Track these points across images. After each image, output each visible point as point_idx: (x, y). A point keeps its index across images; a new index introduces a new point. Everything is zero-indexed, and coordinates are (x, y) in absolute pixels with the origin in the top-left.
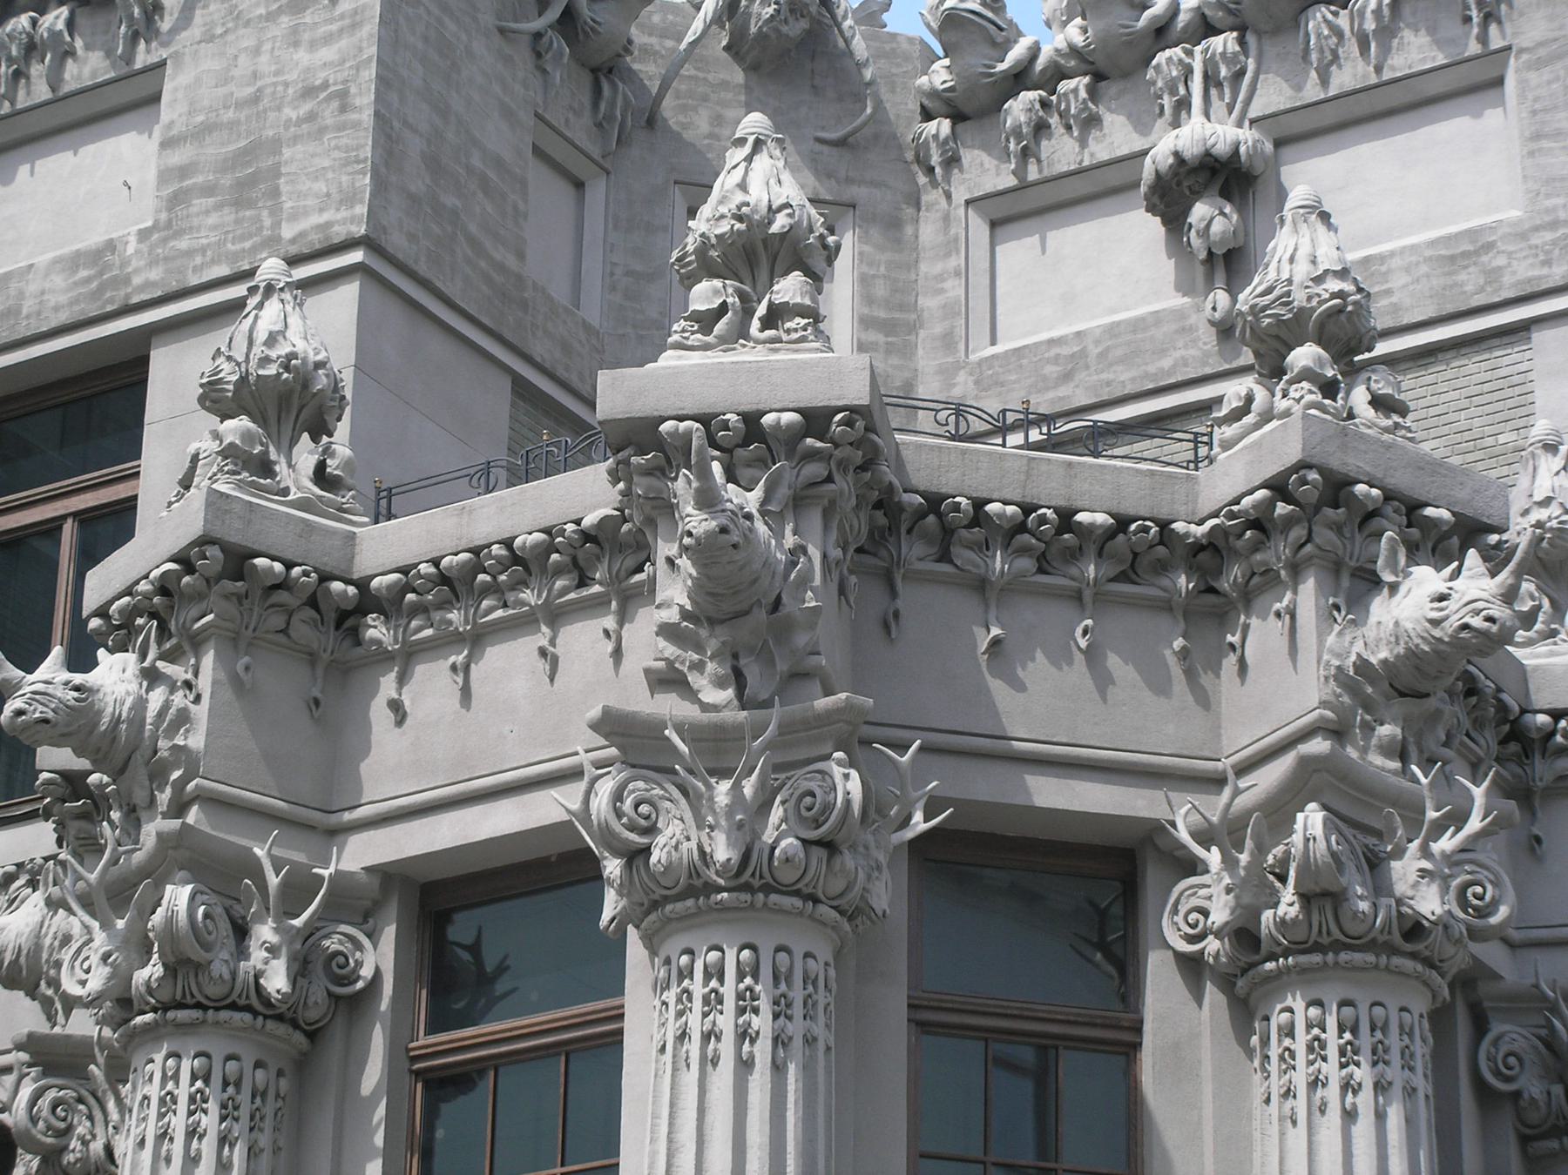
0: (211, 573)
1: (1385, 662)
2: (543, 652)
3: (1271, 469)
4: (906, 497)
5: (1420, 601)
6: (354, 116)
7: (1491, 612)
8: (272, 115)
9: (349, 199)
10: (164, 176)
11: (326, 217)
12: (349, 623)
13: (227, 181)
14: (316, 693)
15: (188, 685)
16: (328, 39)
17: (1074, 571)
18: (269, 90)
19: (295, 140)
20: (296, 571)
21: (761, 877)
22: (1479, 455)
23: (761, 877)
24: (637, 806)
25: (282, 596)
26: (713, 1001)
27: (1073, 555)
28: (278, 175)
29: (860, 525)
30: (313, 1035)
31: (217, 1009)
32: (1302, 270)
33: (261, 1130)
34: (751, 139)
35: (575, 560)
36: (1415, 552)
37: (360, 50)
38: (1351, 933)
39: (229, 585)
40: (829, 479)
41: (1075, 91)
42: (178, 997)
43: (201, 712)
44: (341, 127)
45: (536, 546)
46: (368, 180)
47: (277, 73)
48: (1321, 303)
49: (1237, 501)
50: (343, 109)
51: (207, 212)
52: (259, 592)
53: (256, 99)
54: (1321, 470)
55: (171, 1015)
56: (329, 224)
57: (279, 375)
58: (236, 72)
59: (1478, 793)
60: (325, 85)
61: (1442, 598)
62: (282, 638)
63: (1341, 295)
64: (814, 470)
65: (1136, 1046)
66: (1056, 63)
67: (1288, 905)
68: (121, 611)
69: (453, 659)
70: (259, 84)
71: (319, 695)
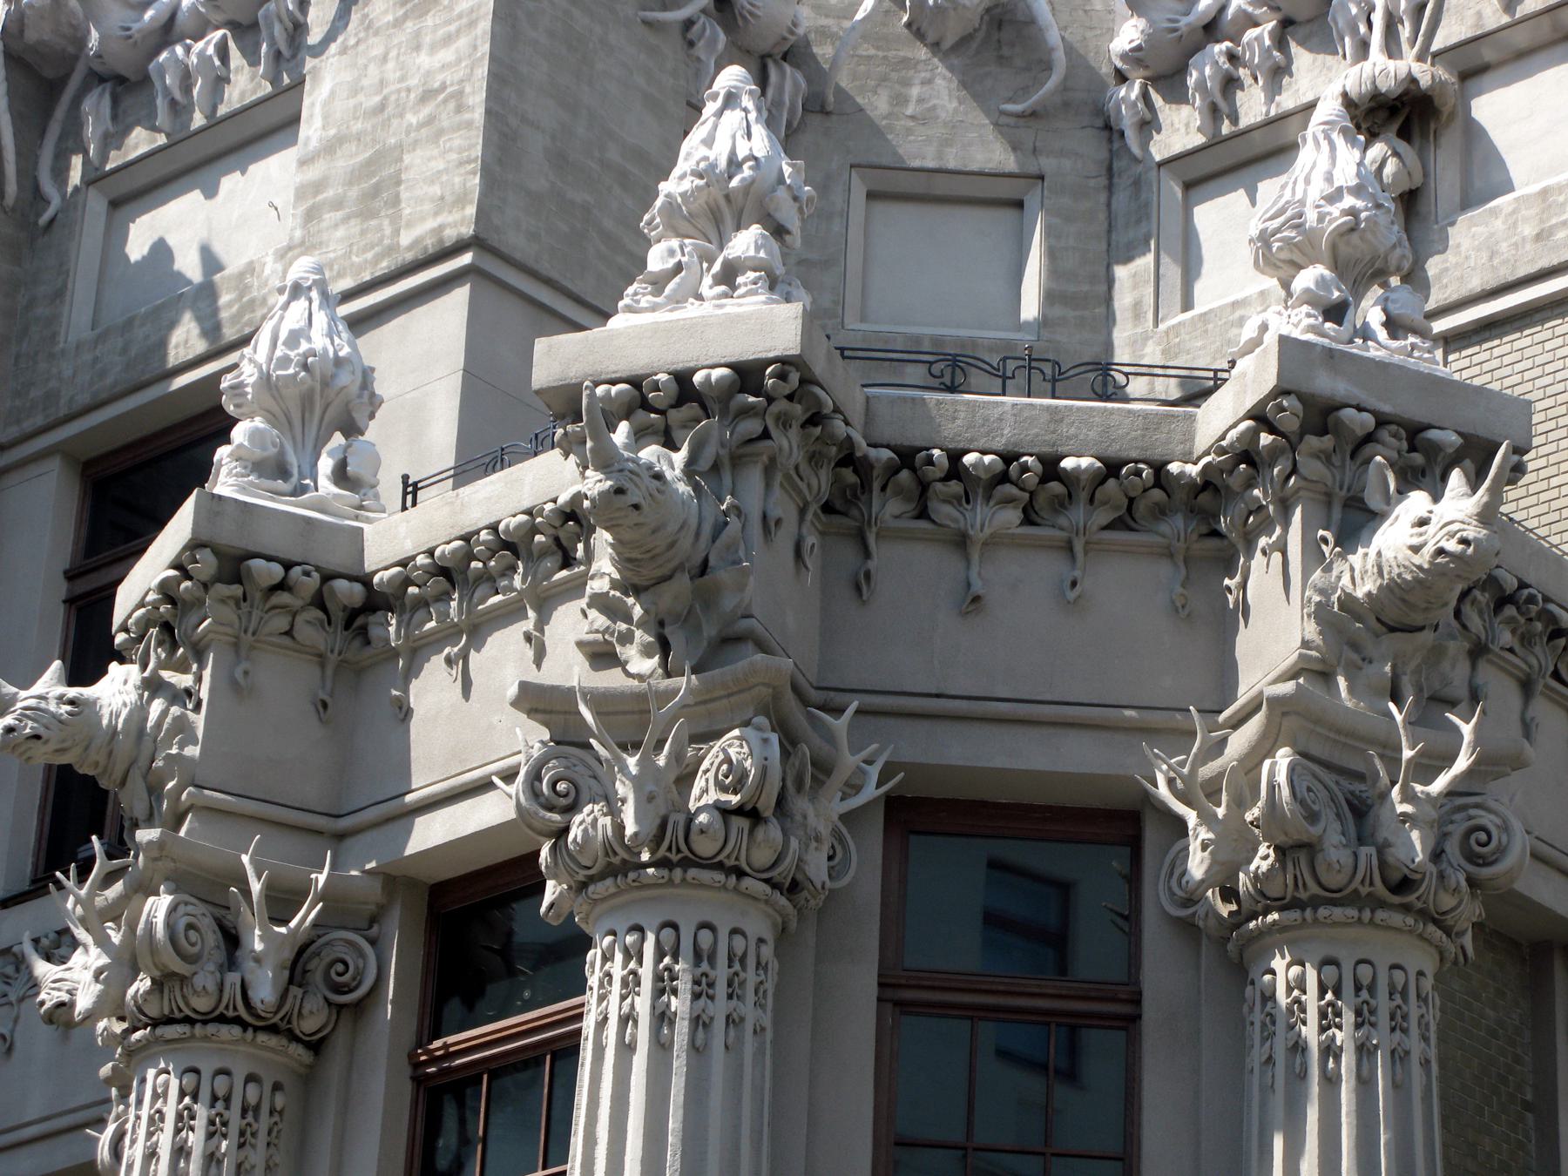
0: (204, 577)
1: (1369, 594)
2: (528, 638)
3: (1249, 402)
4: (873, 452)
5: (1421, 527)
6: (467, 116)
7: (1465, 534)
8: (395, 122)
9: (461, 201)
10: (301, 193)
11: (440, 220)
12: (359, 621)
13: (354, 193)
14: (322, 696)
15: (188, 693)
16: (448, 40)
17: (1062, 521)
18: (393, 98)
19: (416, 143)
20: (297, 570)
21: (679, 851)
22: (1476, 370)
23: (679, 851)
24: (554, 785)
25: (283, 598)
26: (631, 983)
27: (1061, 505)
28: (399, 183)
29: (821, 482)
30: (316, 1046)
31: (205, 1022)
32: (1317, 189)
33: (253, 1146)
34: (722, 93)
35: (557, 540)
36: (1411, 478)
37: (475, 48)
38: (1334, 887)
39: (222, 589)
40: (766, 435)
41: (1259, 39)
42: (166, 1012)
43: (199, 721)
44: (458, 128)
45: (519, 526)
46: (477, 180)
47: (402, 79)
48: (1330, 222)
49: (1223, 437)
50: (460, 109)
51: (336, 226)
52: (258, 595)
53: (382, 107)
54: (1301, 397)
55: (159, 1031)
56: (441, 228)
57: (297, 374)
58: (365, 82)
59: (1467, 729)
60: (443, 87)
61: (1423, 522)
62: (286, 641)
63: (1353, 212)
64: (752, 426)
65: (1136, 1018)
66: (1245, 12)
67: (1263, 860)
68: (137, 622)
69: (447, 651)
70: (385, 91)
71: (326, 698)
